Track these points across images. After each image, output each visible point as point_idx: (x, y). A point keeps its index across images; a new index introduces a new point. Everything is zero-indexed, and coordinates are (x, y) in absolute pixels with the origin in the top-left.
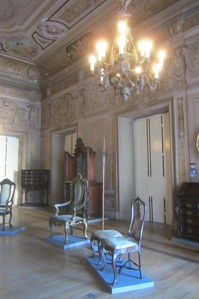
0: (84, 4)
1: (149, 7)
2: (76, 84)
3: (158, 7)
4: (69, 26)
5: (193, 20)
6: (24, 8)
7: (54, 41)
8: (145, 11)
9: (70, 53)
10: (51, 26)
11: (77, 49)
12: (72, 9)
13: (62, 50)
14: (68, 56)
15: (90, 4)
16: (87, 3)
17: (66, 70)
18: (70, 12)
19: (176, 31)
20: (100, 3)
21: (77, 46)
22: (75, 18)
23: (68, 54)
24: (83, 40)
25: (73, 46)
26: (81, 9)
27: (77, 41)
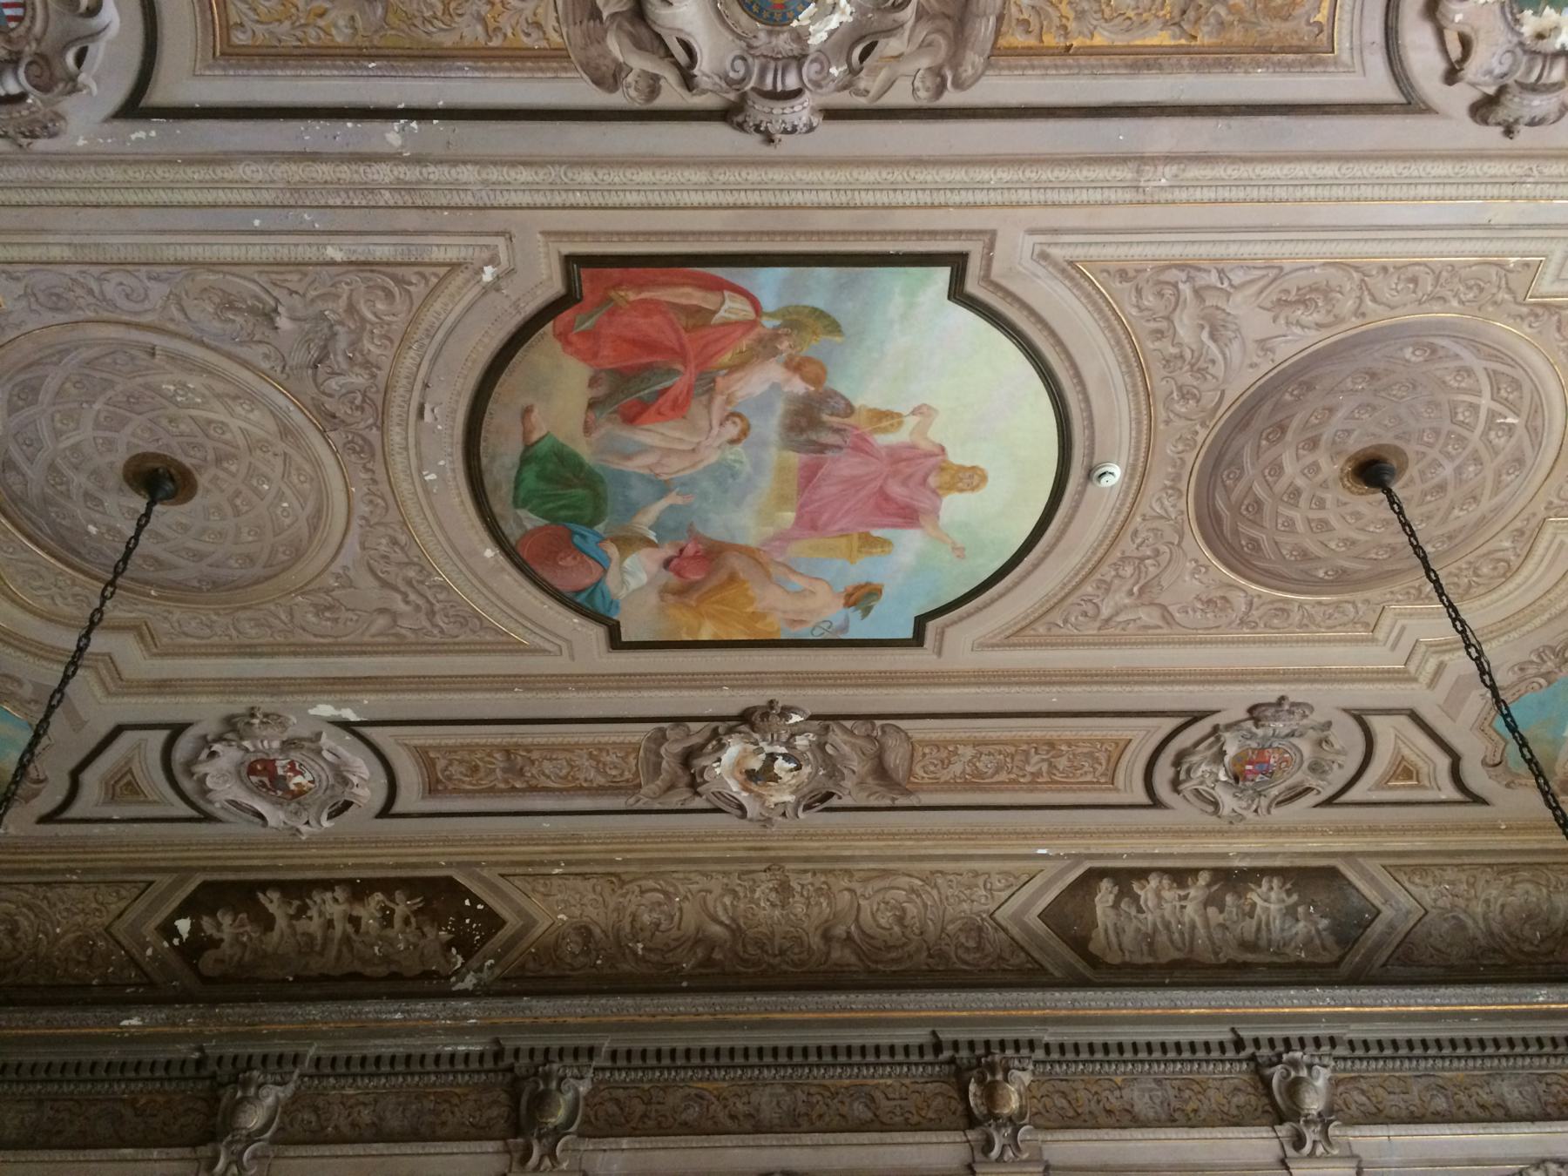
0: (614, 772)
1: (848, 933)
2: (175, 1152)
3: (893, 955)
4: (410, 798)
5: (1076, 1090)
6: (319, 610)
7: (208, 818)
8: (827, 937)
9: (206, 922)
10: (325, 754)
11: (281, 923)
12: (535, 755)
13: (163, 880)
14: (168, 930)
15: (639, 786)
16: (627, 775)
17: (135, 1022)
18: (509, 759)
19: (1006, 1111)
20: (679, 806)
21: (302, 911)
22: (492, 791)
23: (184, 925)
24: (379, 896)
25: (272, 902)
26: (575, 779)
27: (328, 885)
